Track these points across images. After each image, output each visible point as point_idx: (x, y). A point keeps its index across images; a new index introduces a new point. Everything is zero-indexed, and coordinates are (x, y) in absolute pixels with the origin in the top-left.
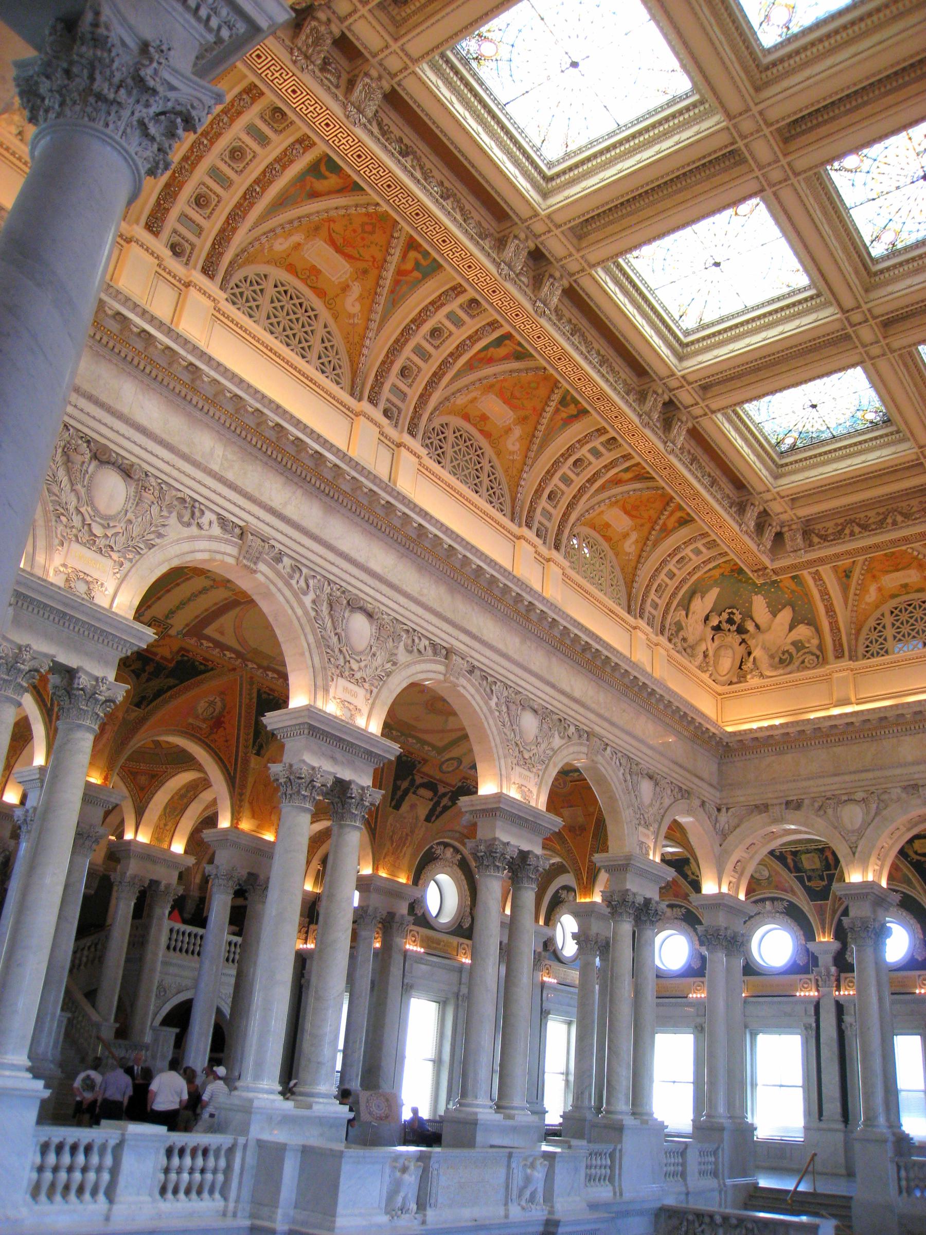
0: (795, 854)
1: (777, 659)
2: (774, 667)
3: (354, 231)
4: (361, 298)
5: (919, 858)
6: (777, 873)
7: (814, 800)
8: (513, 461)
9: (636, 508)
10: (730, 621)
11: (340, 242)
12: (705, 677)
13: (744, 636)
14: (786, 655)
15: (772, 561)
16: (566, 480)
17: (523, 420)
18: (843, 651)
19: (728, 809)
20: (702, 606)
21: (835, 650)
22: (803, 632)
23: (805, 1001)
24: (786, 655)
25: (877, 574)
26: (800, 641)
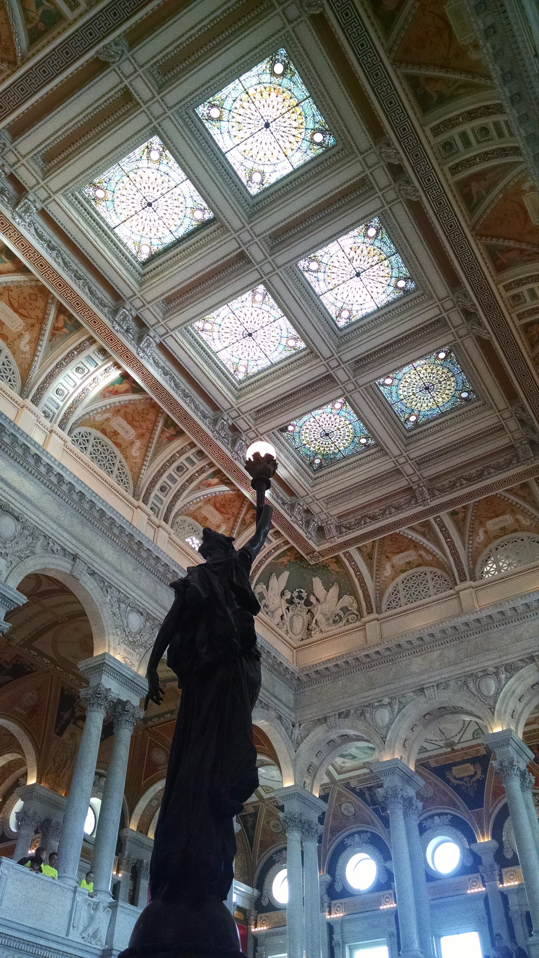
0: (370, 789)
1: (331, 621)
3: (25, 298)
4: (30, 342)
5: (457, 782)
6: (360, 808)
7: (356, 710)
8: (135, 463)
9: (223, 506)
10: (300, 597)
11: (16, 305)
16: (171, 478)
17: (141, 436)
19: (300, 725)
21: (367, 608)
22: (347, 600)
23: (387, 912)
25: (390, 555)
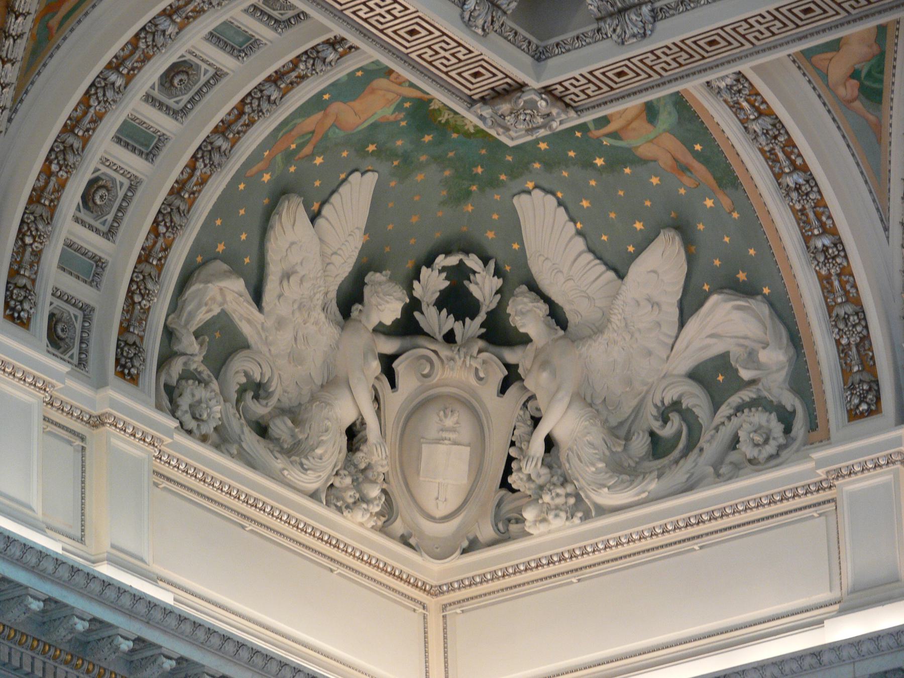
1: (640, 444)
2: (624, 470)
10: (456, 300)
12: (357, 525)
13: (512, 356)
14: (675, 420)
15: (540, 56)
18: (875, 385)
20: (315, 248)
24: (675, 418)
26: (723, 362)
